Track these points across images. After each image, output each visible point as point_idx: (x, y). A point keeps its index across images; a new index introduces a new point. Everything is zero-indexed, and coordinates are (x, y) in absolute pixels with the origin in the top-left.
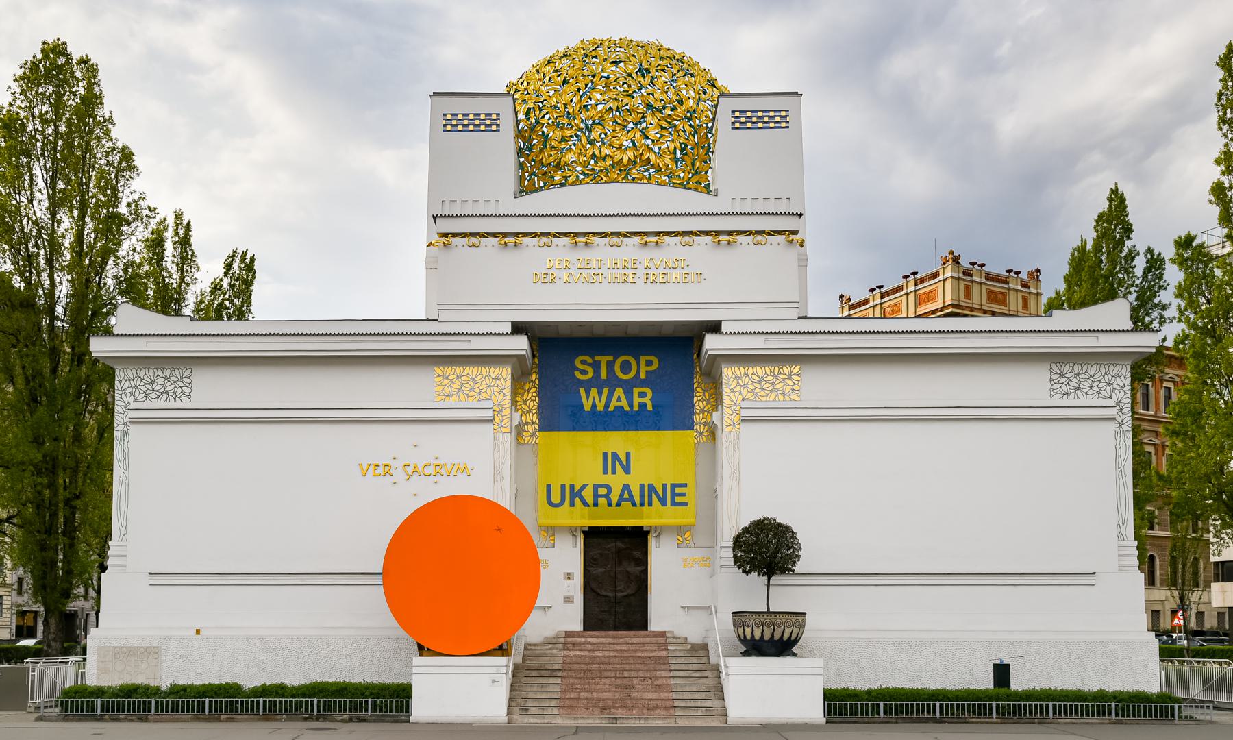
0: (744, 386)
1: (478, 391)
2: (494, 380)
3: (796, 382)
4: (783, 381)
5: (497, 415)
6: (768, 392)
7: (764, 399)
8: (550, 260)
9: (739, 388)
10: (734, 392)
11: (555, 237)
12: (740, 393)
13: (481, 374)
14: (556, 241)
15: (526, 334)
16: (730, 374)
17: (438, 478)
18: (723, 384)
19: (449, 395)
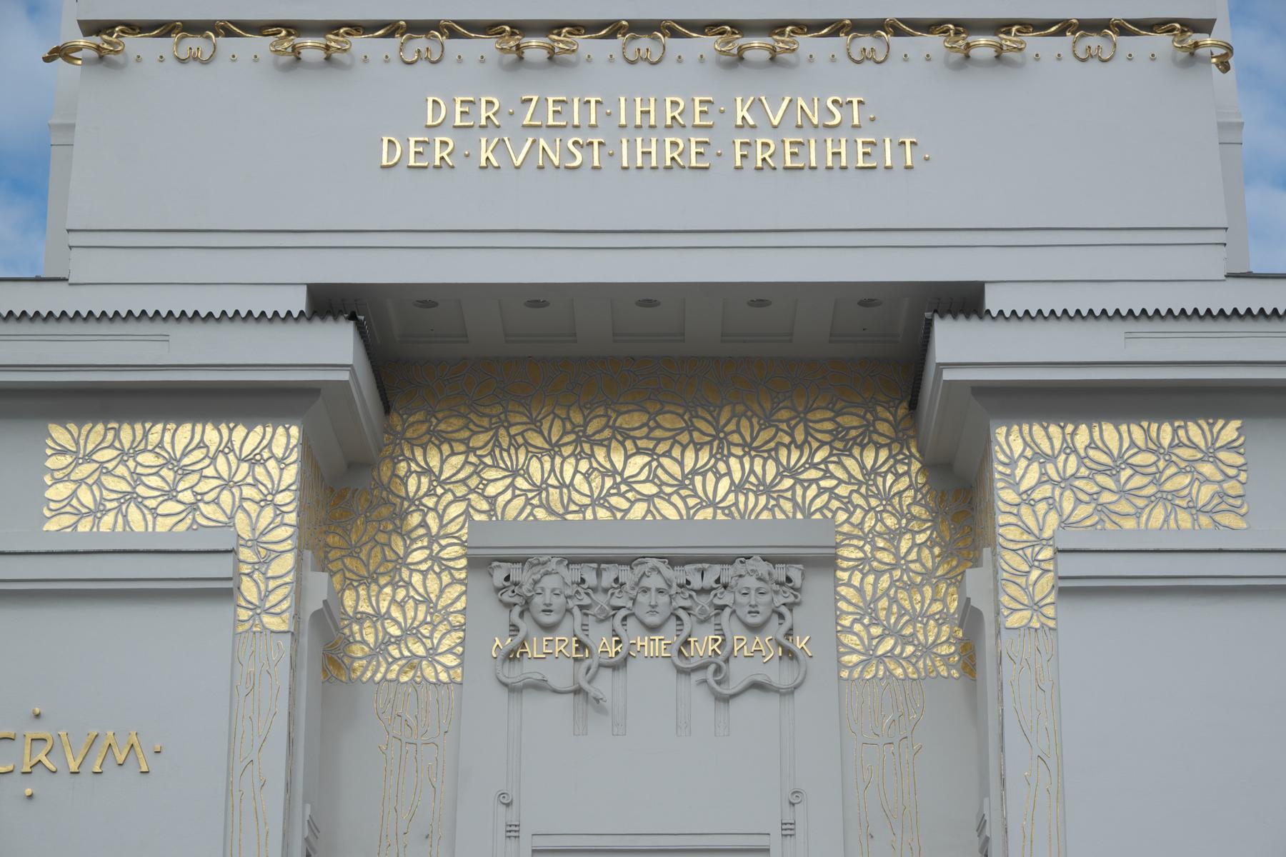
0: (1066, 482)
1: (187, 497)
2: (245, 467)
3: (1231, 472)
4: (1189, 467)
5: (247, 574)
6: (1141, 503)
7: (1129, 524)
9: (1046, 490)
10: (1032, 504)
11: (453, 34)
13: (202, 445)
14: (453, 45)
15: (352, 317)
16: (1018, 447)
18: (997, 476)
19: (91, 512)
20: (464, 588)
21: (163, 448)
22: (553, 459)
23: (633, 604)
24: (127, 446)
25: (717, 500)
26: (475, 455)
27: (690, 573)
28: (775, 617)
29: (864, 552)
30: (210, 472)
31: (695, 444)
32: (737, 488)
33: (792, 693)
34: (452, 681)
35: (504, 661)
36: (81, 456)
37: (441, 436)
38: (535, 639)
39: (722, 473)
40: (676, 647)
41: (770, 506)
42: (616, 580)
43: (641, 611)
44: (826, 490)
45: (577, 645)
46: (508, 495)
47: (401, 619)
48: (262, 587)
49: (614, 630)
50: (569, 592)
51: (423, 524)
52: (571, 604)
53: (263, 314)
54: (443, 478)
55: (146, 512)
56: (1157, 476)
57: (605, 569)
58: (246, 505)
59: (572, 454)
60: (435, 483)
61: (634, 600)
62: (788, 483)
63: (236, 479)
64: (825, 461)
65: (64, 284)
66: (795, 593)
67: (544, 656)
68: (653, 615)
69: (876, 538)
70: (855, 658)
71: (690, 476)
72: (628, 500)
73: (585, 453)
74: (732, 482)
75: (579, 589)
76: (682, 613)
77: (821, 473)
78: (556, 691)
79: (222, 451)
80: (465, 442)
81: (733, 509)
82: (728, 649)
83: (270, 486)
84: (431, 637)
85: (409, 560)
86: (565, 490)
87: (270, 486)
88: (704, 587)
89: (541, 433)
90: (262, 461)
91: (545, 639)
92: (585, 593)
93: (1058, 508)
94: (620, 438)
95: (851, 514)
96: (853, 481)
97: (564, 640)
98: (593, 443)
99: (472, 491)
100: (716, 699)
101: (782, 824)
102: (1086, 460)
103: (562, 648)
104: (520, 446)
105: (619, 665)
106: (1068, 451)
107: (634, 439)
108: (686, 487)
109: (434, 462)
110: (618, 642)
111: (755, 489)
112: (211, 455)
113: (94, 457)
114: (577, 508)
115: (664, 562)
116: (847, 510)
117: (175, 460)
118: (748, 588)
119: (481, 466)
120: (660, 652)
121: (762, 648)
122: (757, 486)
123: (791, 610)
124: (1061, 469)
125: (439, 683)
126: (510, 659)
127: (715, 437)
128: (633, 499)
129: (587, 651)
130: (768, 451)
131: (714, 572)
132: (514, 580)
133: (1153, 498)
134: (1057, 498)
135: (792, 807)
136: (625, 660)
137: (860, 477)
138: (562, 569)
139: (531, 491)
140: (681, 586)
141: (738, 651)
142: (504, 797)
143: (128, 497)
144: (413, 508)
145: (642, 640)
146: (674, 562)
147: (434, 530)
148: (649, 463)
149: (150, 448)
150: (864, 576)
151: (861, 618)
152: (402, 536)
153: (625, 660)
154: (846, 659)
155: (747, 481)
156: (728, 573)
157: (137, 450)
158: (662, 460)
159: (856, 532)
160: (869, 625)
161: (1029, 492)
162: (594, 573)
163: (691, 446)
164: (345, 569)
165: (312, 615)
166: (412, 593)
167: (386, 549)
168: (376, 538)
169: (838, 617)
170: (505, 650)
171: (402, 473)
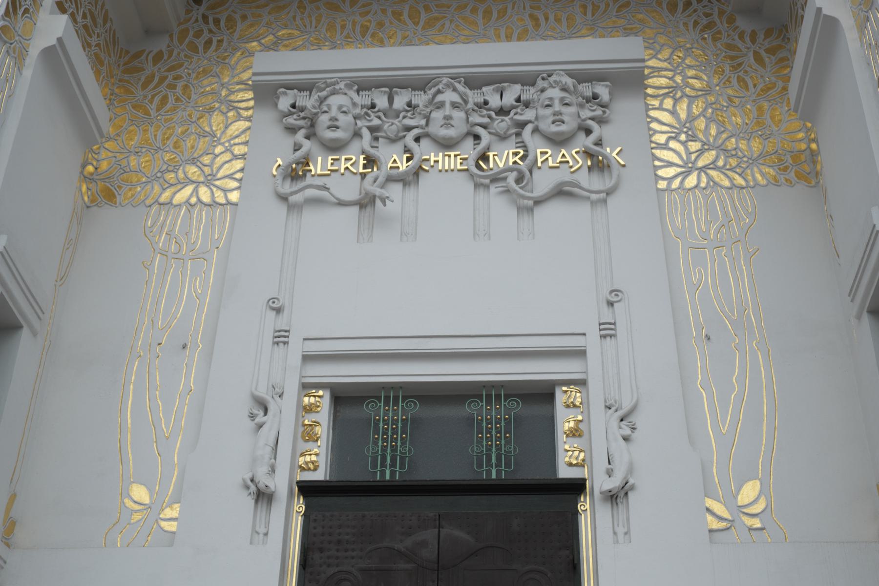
28: (582, 135)
29: (675, 82)
33: (605, 201)
34: (229, 203)
35: (284, 178)
38: (320, 159)
42: (409, 104)
43: (433, 129)
45: (365, 162)
50: (358, 111)
57: (397, 93)
66: (603, 109)
67: (329, 172)
68: (447, 128)
69: (686, 70)
70: (670, 172)
75: (369, 112)
78: (342, 204)
82: (530, 157)
84: (210, 166)
88: (503, 106)
91: (330, 158)
92: (376, 117)
95: (659, 52)
97: (351, 159)
100: (520, 209)
101: (600, 324)
103: (348, 165)
110: (408, 160)
115: (460, 82)
118: (551, 99)
121: (568, 158)
125: (213, 204)
129: (375, 169)
132: (301, 104)
135: (611, 308)
140: (476, 104)
141: (542, 162)
142: (274, 302)
145: (436, 155)
146: (474, 82)
150: (676, 101)
151: (676, 136)
154: (660, 173)
156: (529, 94)
160: (686, 142)
165: (42, 50)
169: (651, 136)
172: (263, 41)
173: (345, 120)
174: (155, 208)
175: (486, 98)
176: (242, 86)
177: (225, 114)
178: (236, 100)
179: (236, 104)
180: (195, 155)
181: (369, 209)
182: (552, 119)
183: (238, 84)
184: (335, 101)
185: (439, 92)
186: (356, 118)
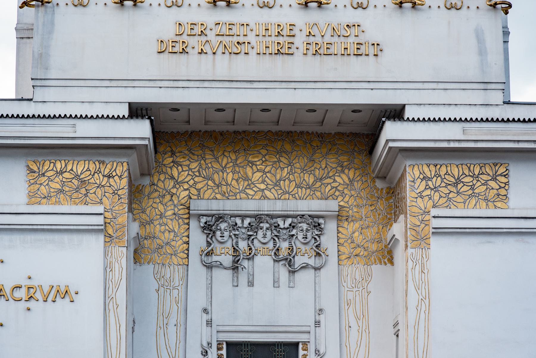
1: (83, 191)
2: (106, 179)
8: (179, 24)
9: (428, 192)
10: (422, 197)
12: (430, 199)
15: (149, 118)
16: (417, 173)
17: (32, 304)
19: (45, 197)
20: (188, 226)
21: (72, 170)
22: (223, 174)
23: (256, 234)
24: (58, 170)
25: (290, 191)
26: (192, 172)
27: (280, 222)
28: (313, 240)
30: (92, 181)
31: (281, 168)
32: (297, 186)
33: (320, 269)
35: (205, 256)
36: (41, 174)
37: (178, 164)
39: (292, 180)
40: (274, 251)
41: (311, 194)
42: (249, 224)
44: (334, 187)
46: (205, 188)
47: (163, 238)
48: (115, 228)
49: (248, 244)
51: (171, 200)
52: (231, 234)
53: (113, 116)
54: (179, 180)
55: (67, 197)
56: (473, 186)
58: (106, 194)
59: (232, 171)
60: (176, 183)
61: (256, 232)
62: (318, 184)
63: (102, 184)
64: (334, 175)
65: (32, 102)
71: (279, 181)
72: (254, 191)
73: (236, 171)
74: (296, 184)
76: (276, 239)
77: (332, 181)
79: (96, 172)
80: (188, 166)
81: (297, 195)
82: (294, 252)
83: (116, 188)
85: (166, 215)
86: (228, 186)
87: (116, 188)
89: (218, 162)
90: (113, 177)
93: (433, 199)
94: (251, 165)
96: (345, 184)
98: (239, 167)
99: (191, 186)
100: (289, 272)
102: (445, 180)
103: (228, 251)
104: (210, 168)
105: (250, 258)
106: (437, 176)
107: (256, 165)
108: (277, 186)
109: (175, 173)
111: (305, 186)
112: (92, 174)
113: (45, 174)
114: (233, 194)
116: (342, 196)
117: (78, 176)
119: (194, 176)
120: (267, 253)
122: (306, 186)
123: (319, 237)
124: (434, 183)
126: (207, 255)
127: (289, 166)
128: (256, 191)
130: (311, 171)
131: (289, 221)
133: (471, 196)
134: (432, 195)
136: (253, 256)
137: (348, 182)
138: (229, 219)
139: (214, 187)
140: (275, 227)
143: (59, 191)
144: (167, 193)
147: (176, 202)
148: (262, 176)
149: (68, 171)
152: (163, 205)
153: (253, 256)
155: (302, 183)
157: (63, 171)
158: (267, 174)
159: (346, 205)
161: (421, 193)
162: (241, 221)
163: (280, 168)
164: (140, 218)
166: (167, 228)
167: (157, 210)
168: (152, 205)
170: (206, 252)
171: (162, 179)
172: (189, 183)
173: (226, 234)
174: (157, 265)
175: (279, 223)
176: (182, 207)
177: (178, 221)
178: (182, 213)
179: (181, 216)
180: (169, 241)
181: (236, 270)
182: (302, 236)
183: (181, 205)
184: (223, 226)
185: (261, 222)
186: (230, 231)
